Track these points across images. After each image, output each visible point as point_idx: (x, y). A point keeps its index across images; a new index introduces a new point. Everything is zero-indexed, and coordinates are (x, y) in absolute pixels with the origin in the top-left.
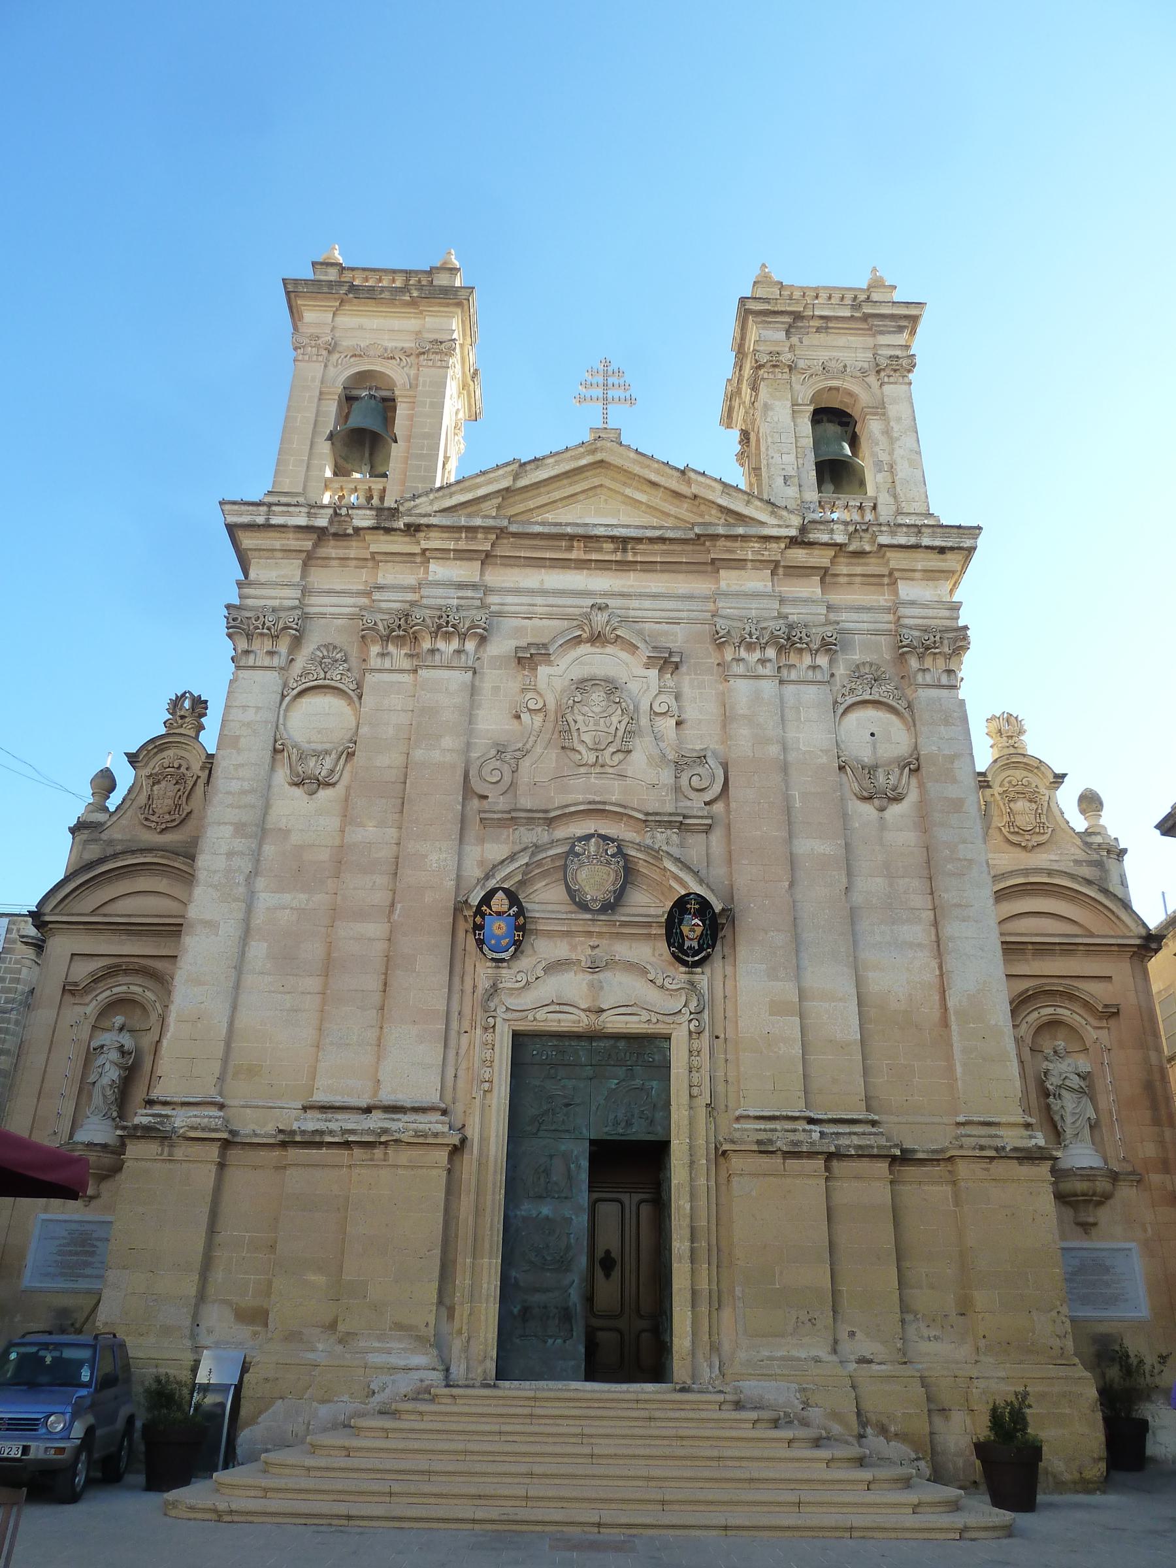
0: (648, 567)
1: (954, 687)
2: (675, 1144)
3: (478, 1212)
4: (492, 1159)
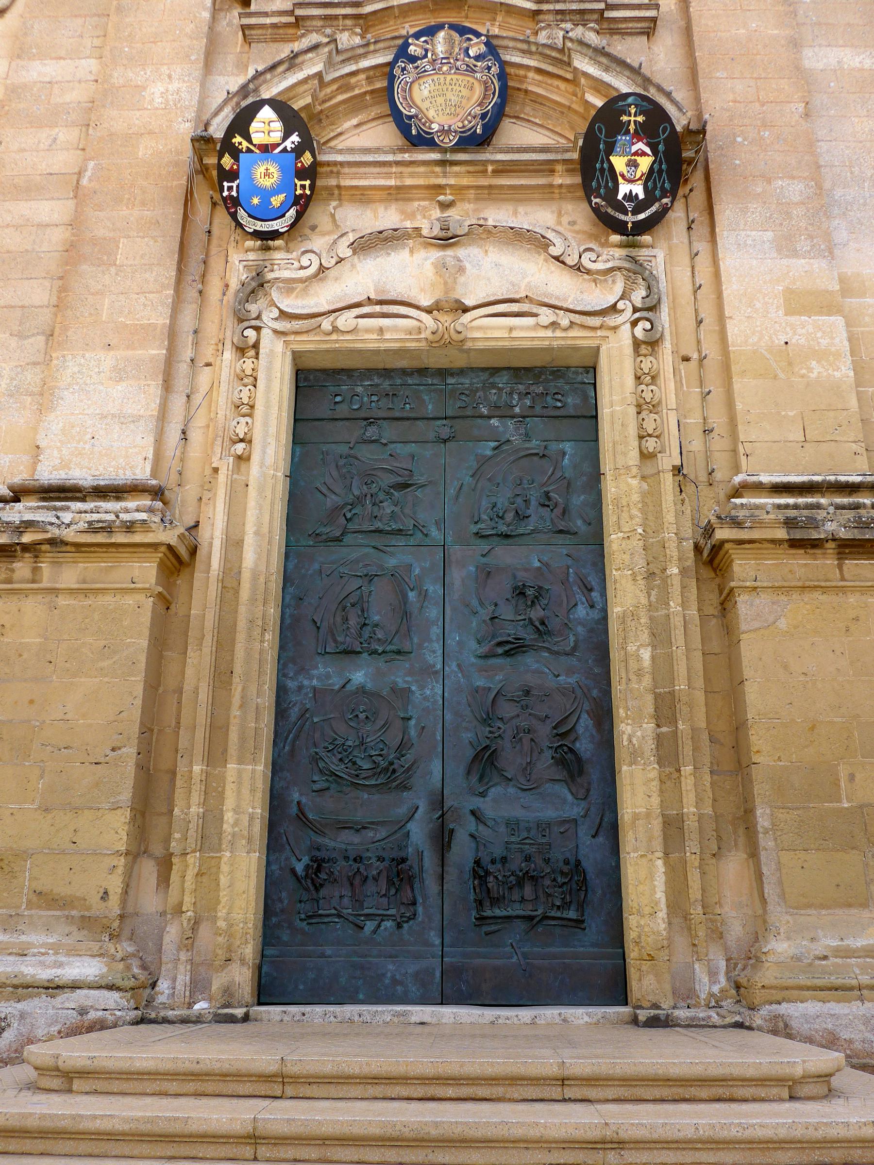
4: (246, 576)
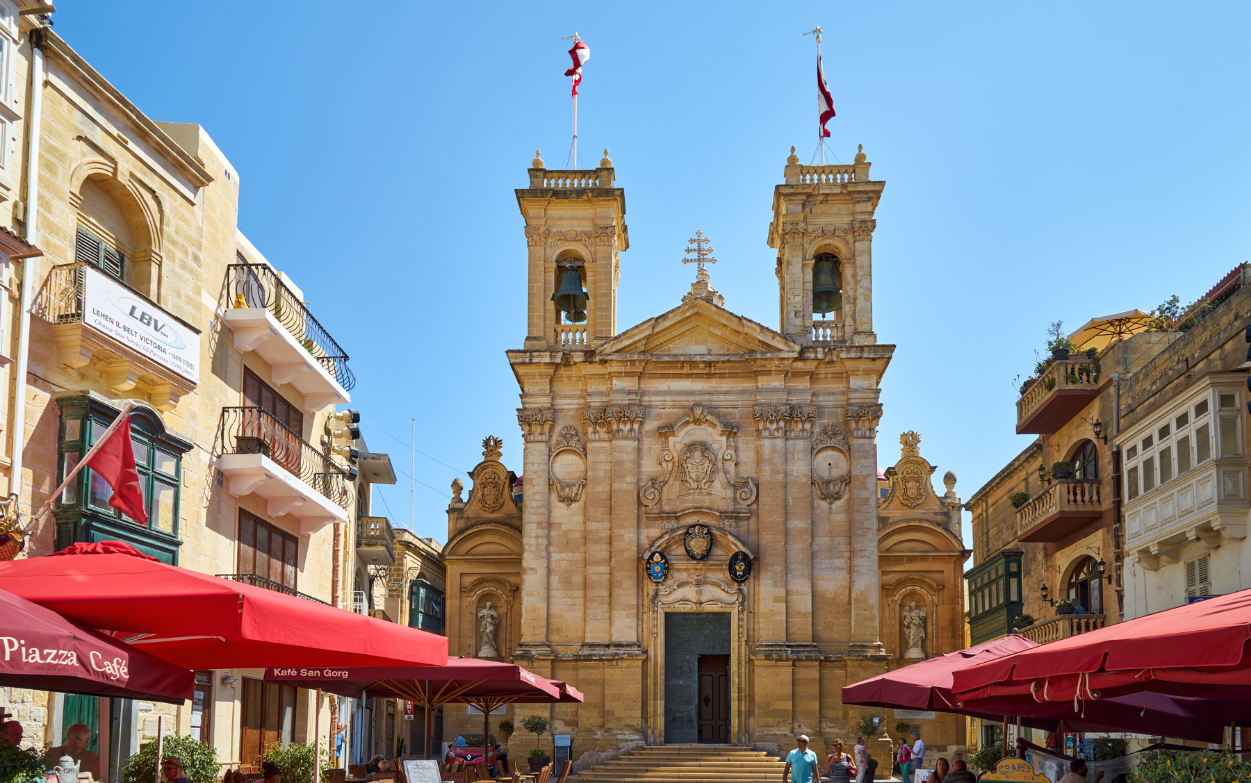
0: (722, 376)
1: (872, 438)
2: (732, 656)
3: (655, 684)
